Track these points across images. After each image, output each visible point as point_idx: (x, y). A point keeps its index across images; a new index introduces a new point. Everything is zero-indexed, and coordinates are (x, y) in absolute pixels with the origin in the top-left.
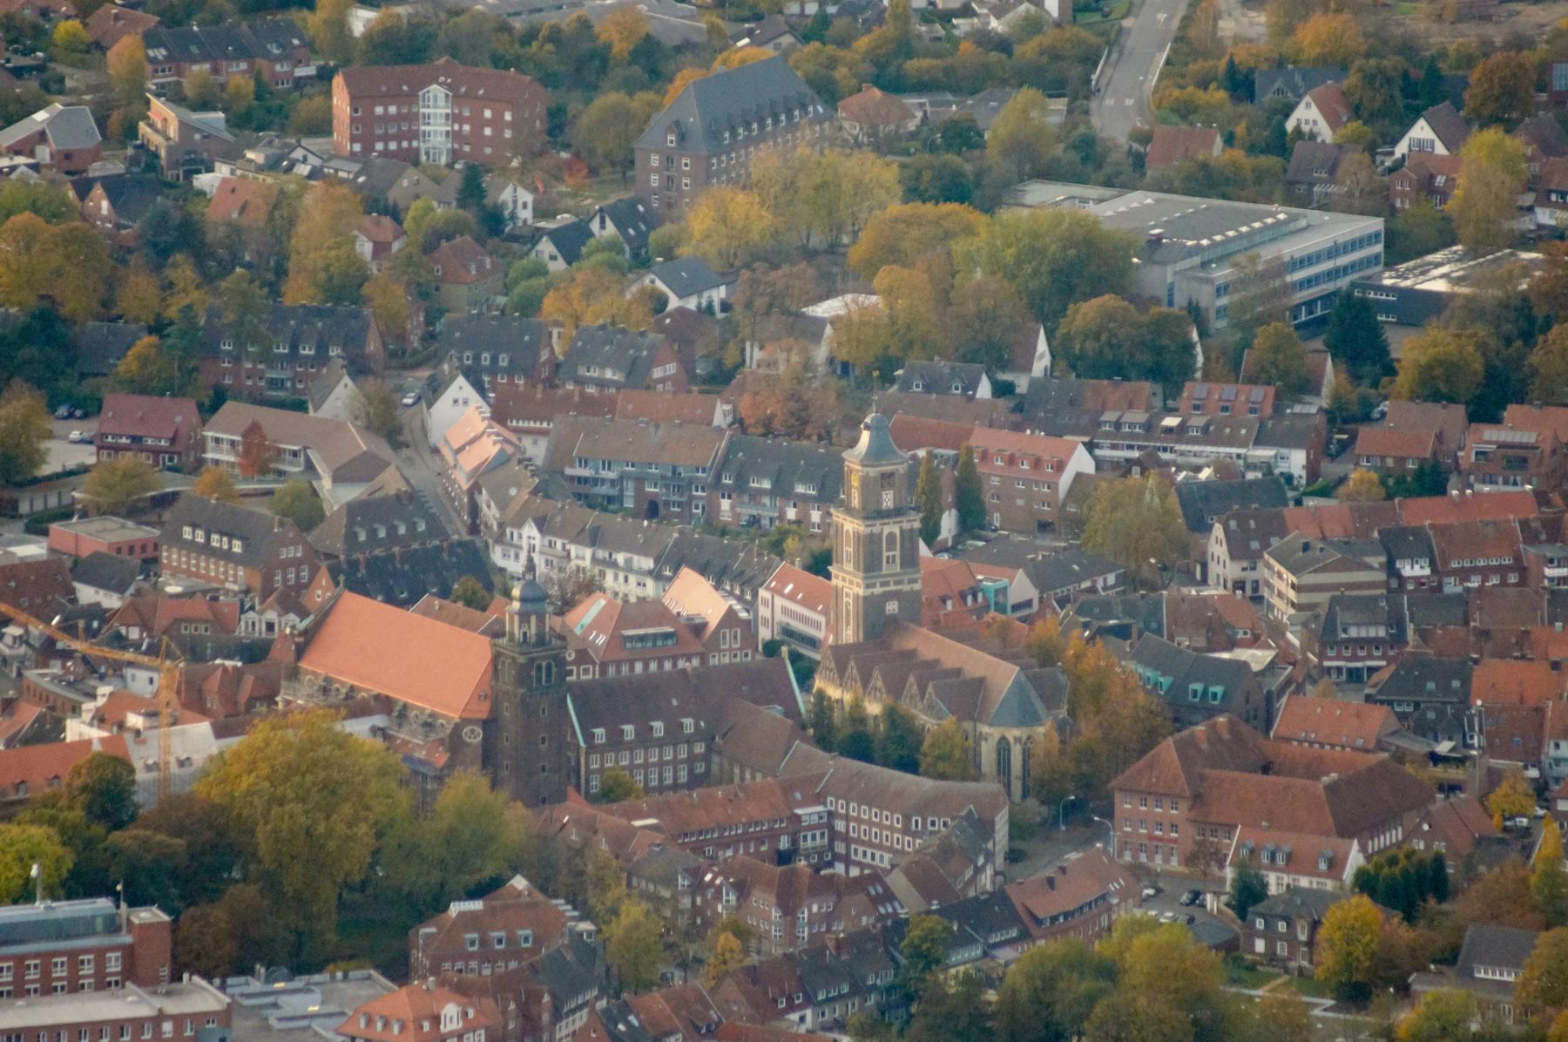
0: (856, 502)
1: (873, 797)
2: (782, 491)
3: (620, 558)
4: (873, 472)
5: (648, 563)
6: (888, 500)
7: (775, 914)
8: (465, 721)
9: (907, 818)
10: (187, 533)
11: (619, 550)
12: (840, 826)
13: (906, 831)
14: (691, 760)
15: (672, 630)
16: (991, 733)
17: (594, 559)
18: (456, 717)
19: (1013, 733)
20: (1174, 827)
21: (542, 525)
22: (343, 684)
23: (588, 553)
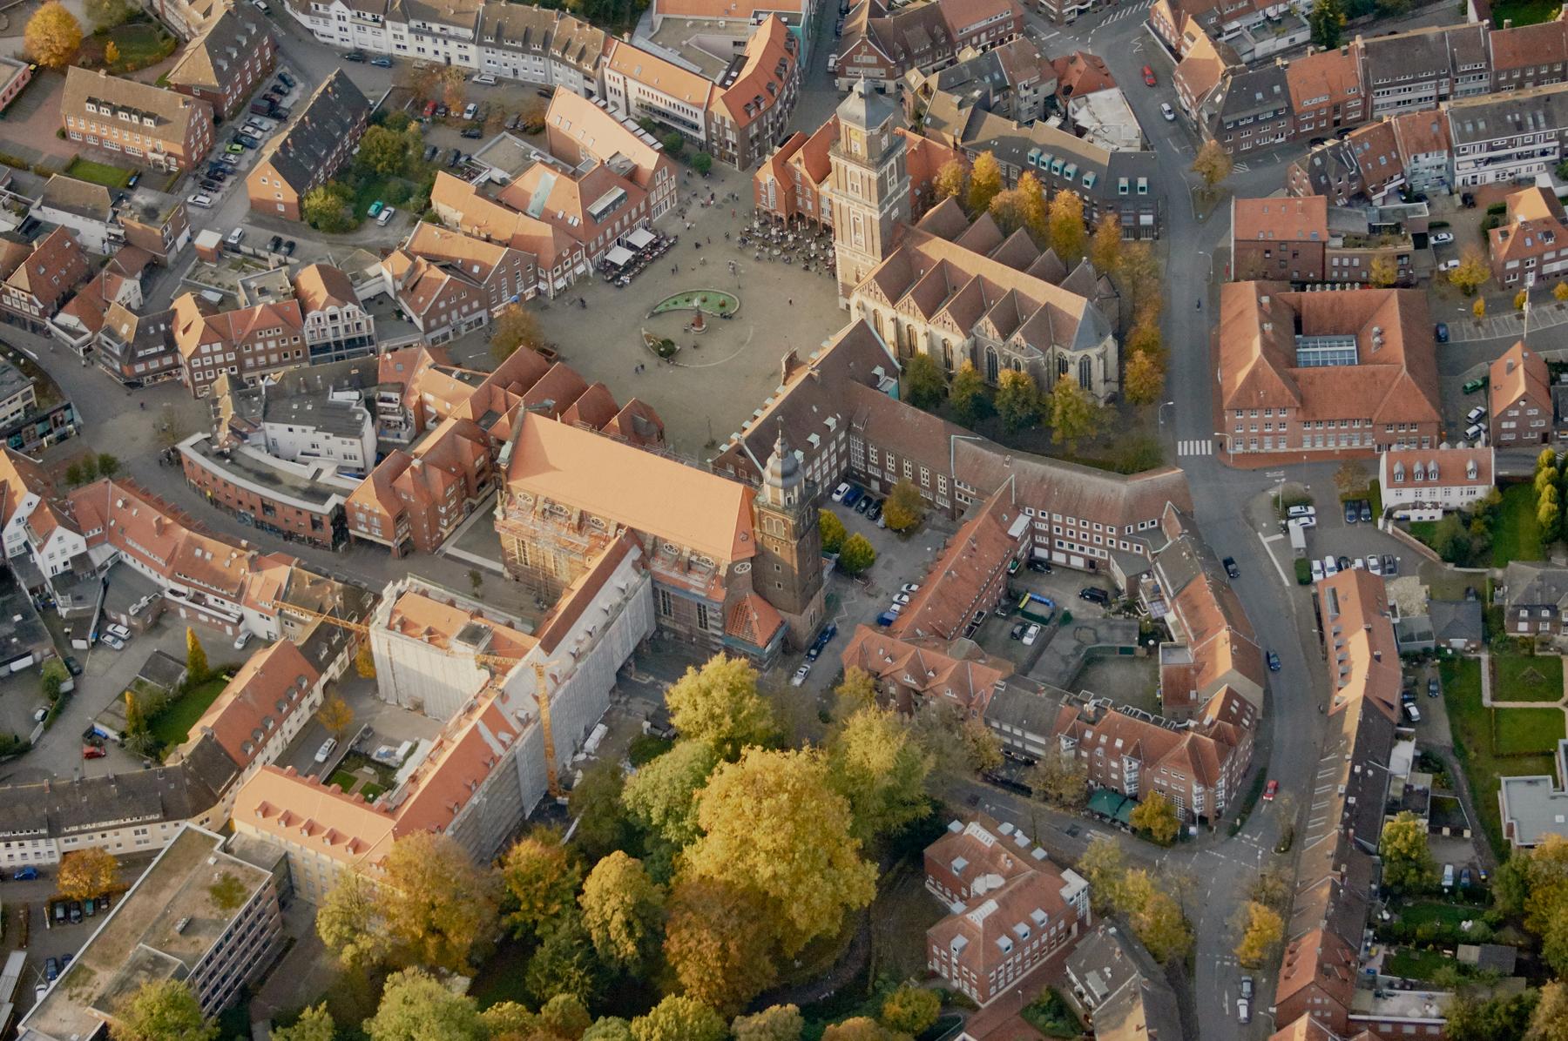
0: (859, 147)
4: (876, 131)
5: (469, 33)
6: (885, 142)
7: (1196, 789)
8: (735, 563)
9: (1121, 529)
12: (1043, 527)
13: (1120, 536)
14: (837, 450)
15: (621, 191)
16: (1073, 355)
18: (727, 560)
19: (1093, 353)
20: (1282, 425)
23: (405, 27)
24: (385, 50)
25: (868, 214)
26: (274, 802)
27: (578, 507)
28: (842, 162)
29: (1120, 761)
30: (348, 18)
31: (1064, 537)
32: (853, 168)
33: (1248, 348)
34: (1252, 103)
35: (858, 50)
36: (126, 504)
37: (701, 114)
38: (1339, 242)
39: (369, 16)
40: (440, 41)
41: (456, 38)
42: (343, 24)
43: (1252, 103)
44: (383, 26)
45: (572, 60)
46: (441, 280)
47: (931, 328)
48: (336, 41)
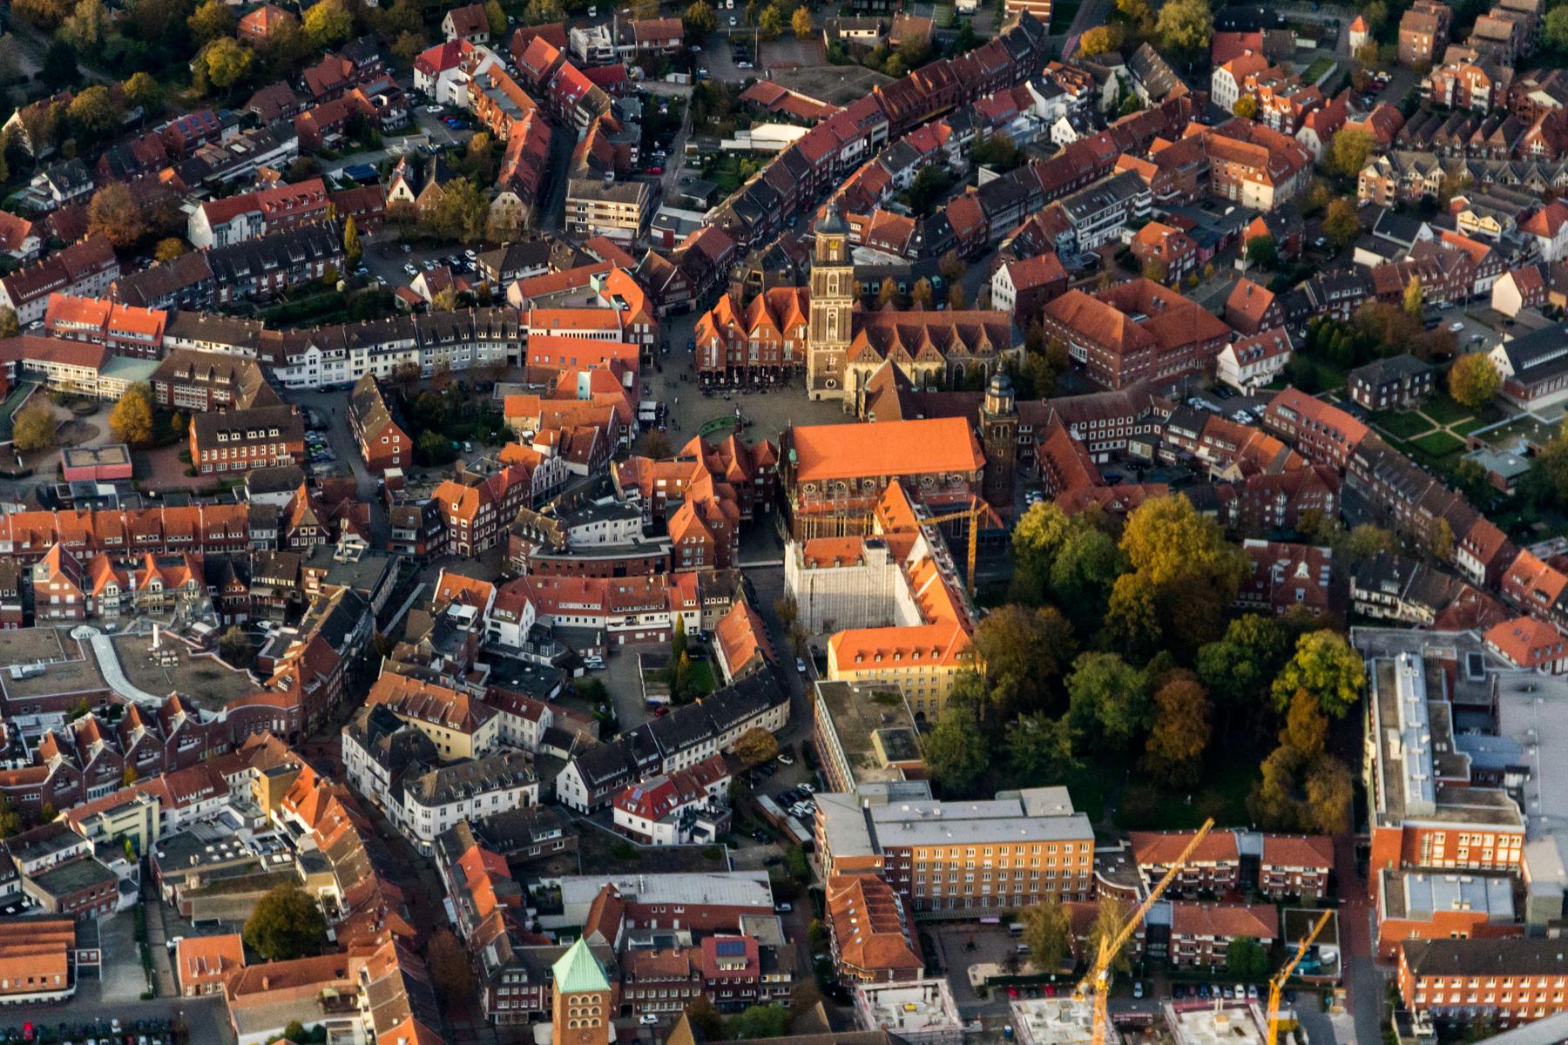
1: (1101, 413)
2: (258, 272)
3: (385, 346)
10: (222, 438)
11: (383, 341)
13: (1136, 423)
17: (370, 354)
21: (321, 347)
22: (847, 480)
23: (366, 351)
24: (346, 379)
25: (842, 306)
26: (865, 647)
27: (853, 476)
28: (824, 270)
29: (1273, 504)
30: (318, 360)
31: (1097, 440)
32: (834, 272)
33: (1108, 318)
34: (939, 238)
35: (674, 280)
36: (546, 583)
37: (619, 333)
38: (1072, 278)
39: (333, 353)
40: (390, 356)
41: (401, 350)
42: (313, 367)
43: (939, 238)
44: (348, 357)
45: (497, 336)
46: (592, 433)
47: (916, 365)
48: (307, 384)
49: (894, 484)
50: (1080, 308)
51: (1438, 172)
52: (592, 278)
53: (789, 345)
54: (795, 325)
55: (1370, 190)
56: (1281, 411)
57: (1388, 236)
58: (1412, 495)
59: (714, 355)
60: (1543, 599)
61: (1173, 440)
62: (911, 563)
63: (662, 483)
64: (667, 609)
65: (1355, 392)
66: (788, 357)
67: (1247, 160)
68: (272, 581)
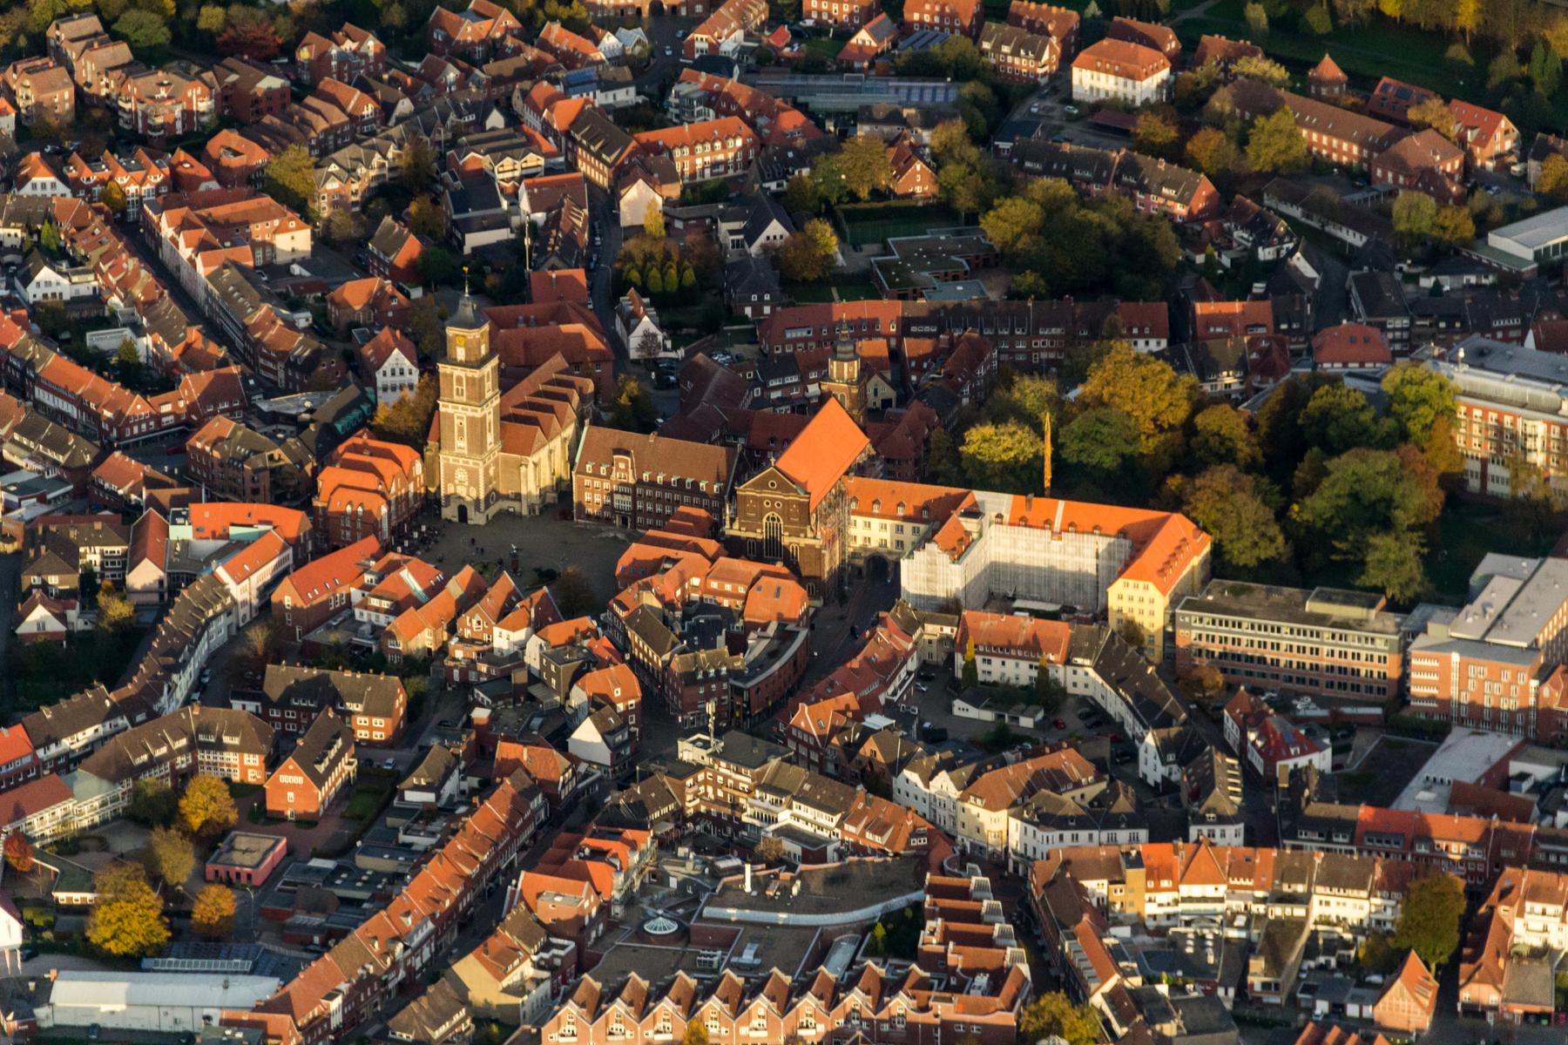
33: (569, 336)
49: (853, 481)
50: (526, 344)
51: (377, 158)
52: (172, 529)
53: (411, 487)
54: (413, 464)
55: (334, 204)
56: (789, 335)
57: (471, 213)
58: (1021, 325)
59: (385, 526)
60: (1262, 331)
61: (775, 395)
62: (1000, 516)
63: (679, 593)
64: (905, 662)
65: (748, 311)
66: (412, 503)
67: (267, 216)
68: (657, 814)
